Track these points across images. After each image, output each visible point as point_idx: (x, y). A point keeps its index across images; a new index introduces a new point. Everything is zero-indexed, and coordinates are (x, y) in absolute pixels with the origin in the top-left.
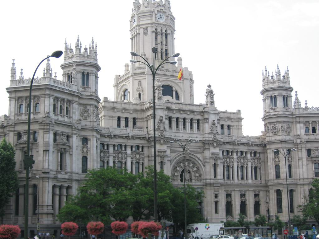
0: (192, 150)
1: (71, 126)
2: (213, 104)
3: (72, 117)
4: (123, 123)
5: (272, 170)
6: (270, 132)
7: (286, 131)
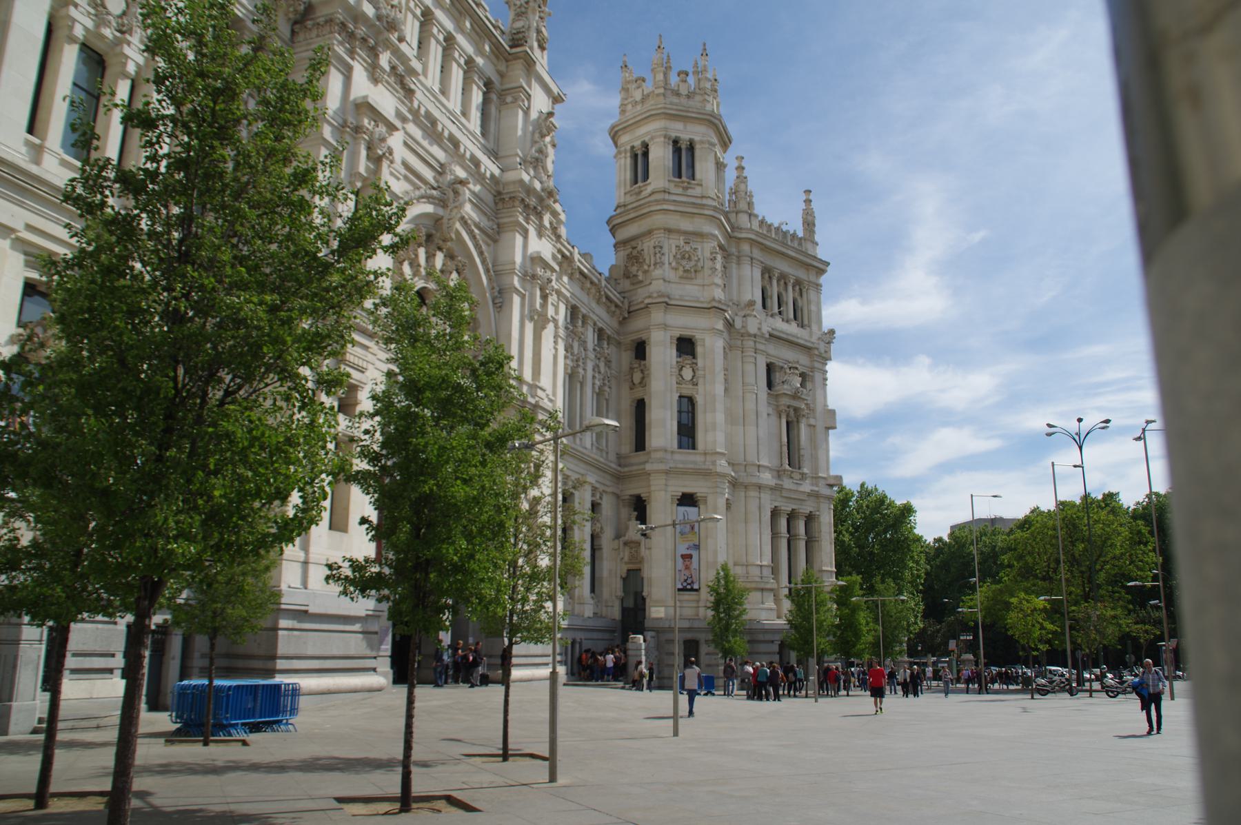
5: (669, 413)
6: (667, 265)
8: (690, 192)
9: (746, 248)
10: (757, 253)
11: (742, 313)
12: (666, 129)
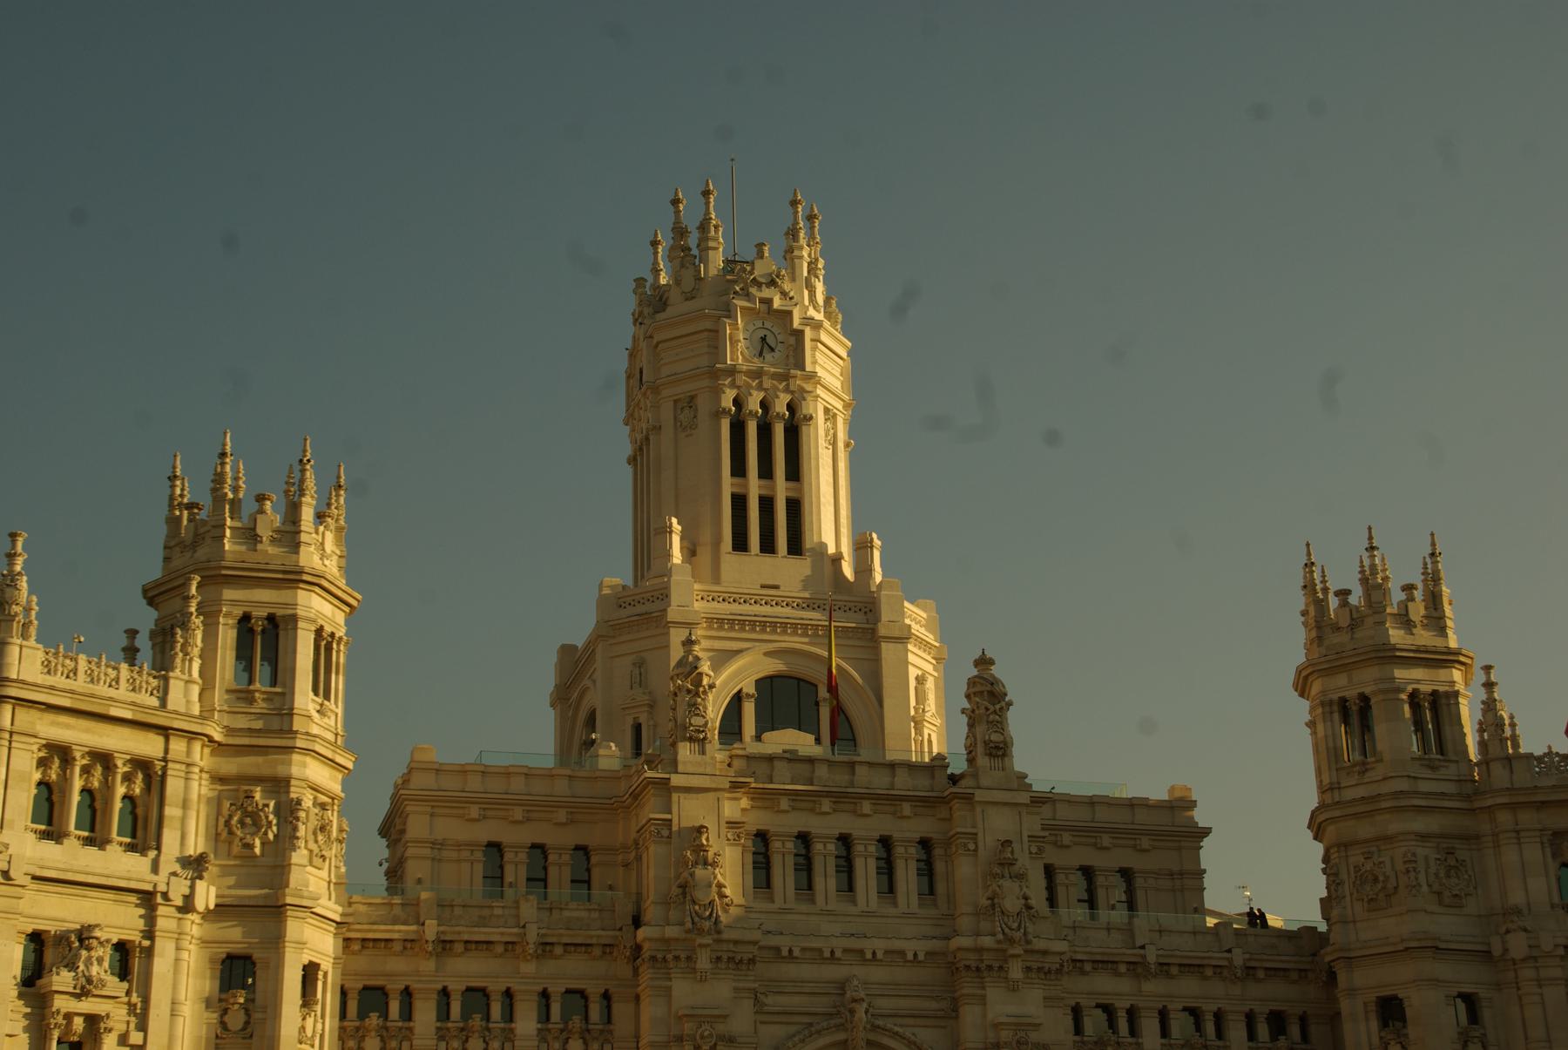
0: (884, 1004)
1: (148, 899)
2: (1004, 755)
3: (158, 848)
4: (515, 871)
6: (1348, 898)
7: (1436, 887)
8: (1370, 776)
9: (1504, 818)
10: (1527, 818)
11: (1503, 930)
12: (1323, 692)
